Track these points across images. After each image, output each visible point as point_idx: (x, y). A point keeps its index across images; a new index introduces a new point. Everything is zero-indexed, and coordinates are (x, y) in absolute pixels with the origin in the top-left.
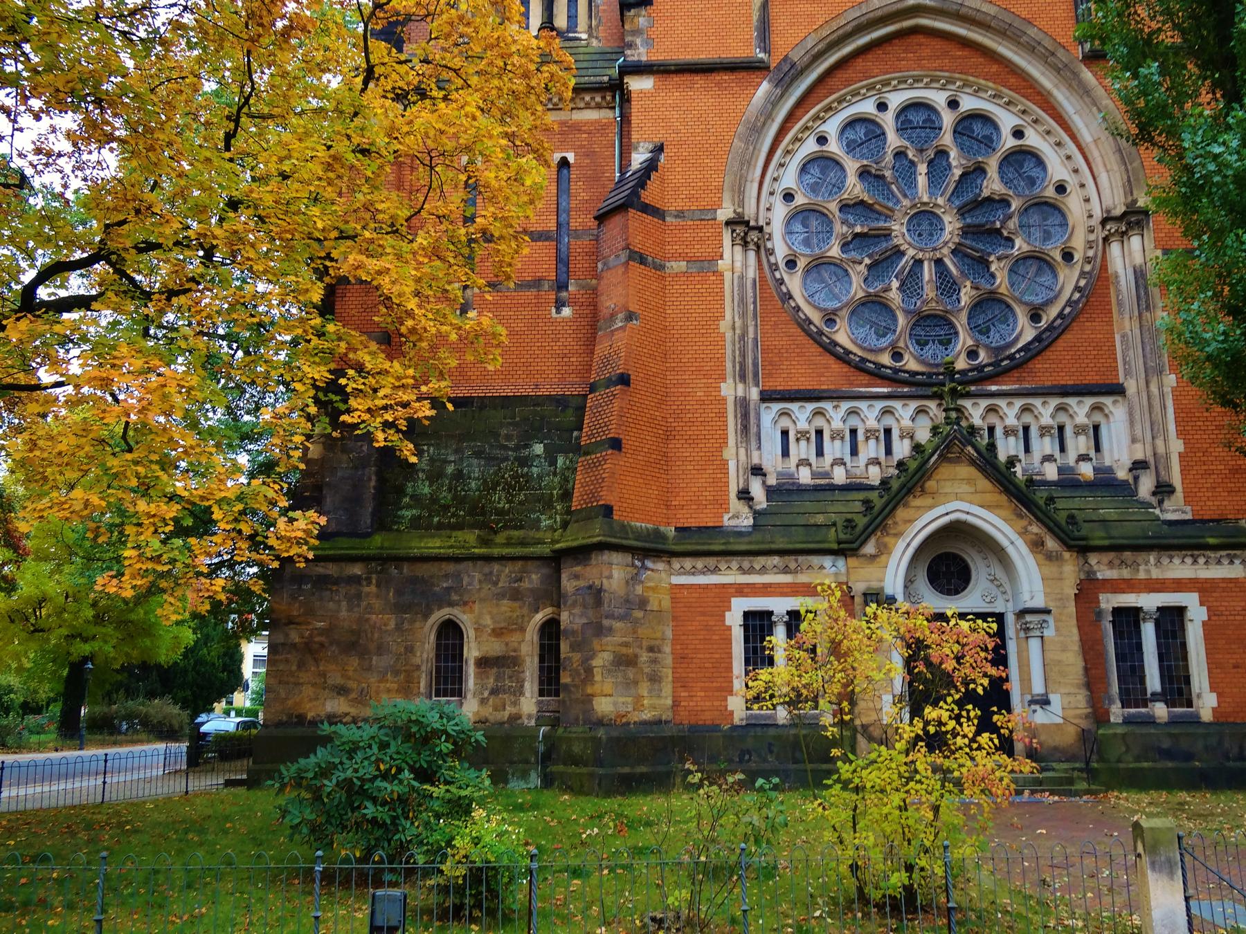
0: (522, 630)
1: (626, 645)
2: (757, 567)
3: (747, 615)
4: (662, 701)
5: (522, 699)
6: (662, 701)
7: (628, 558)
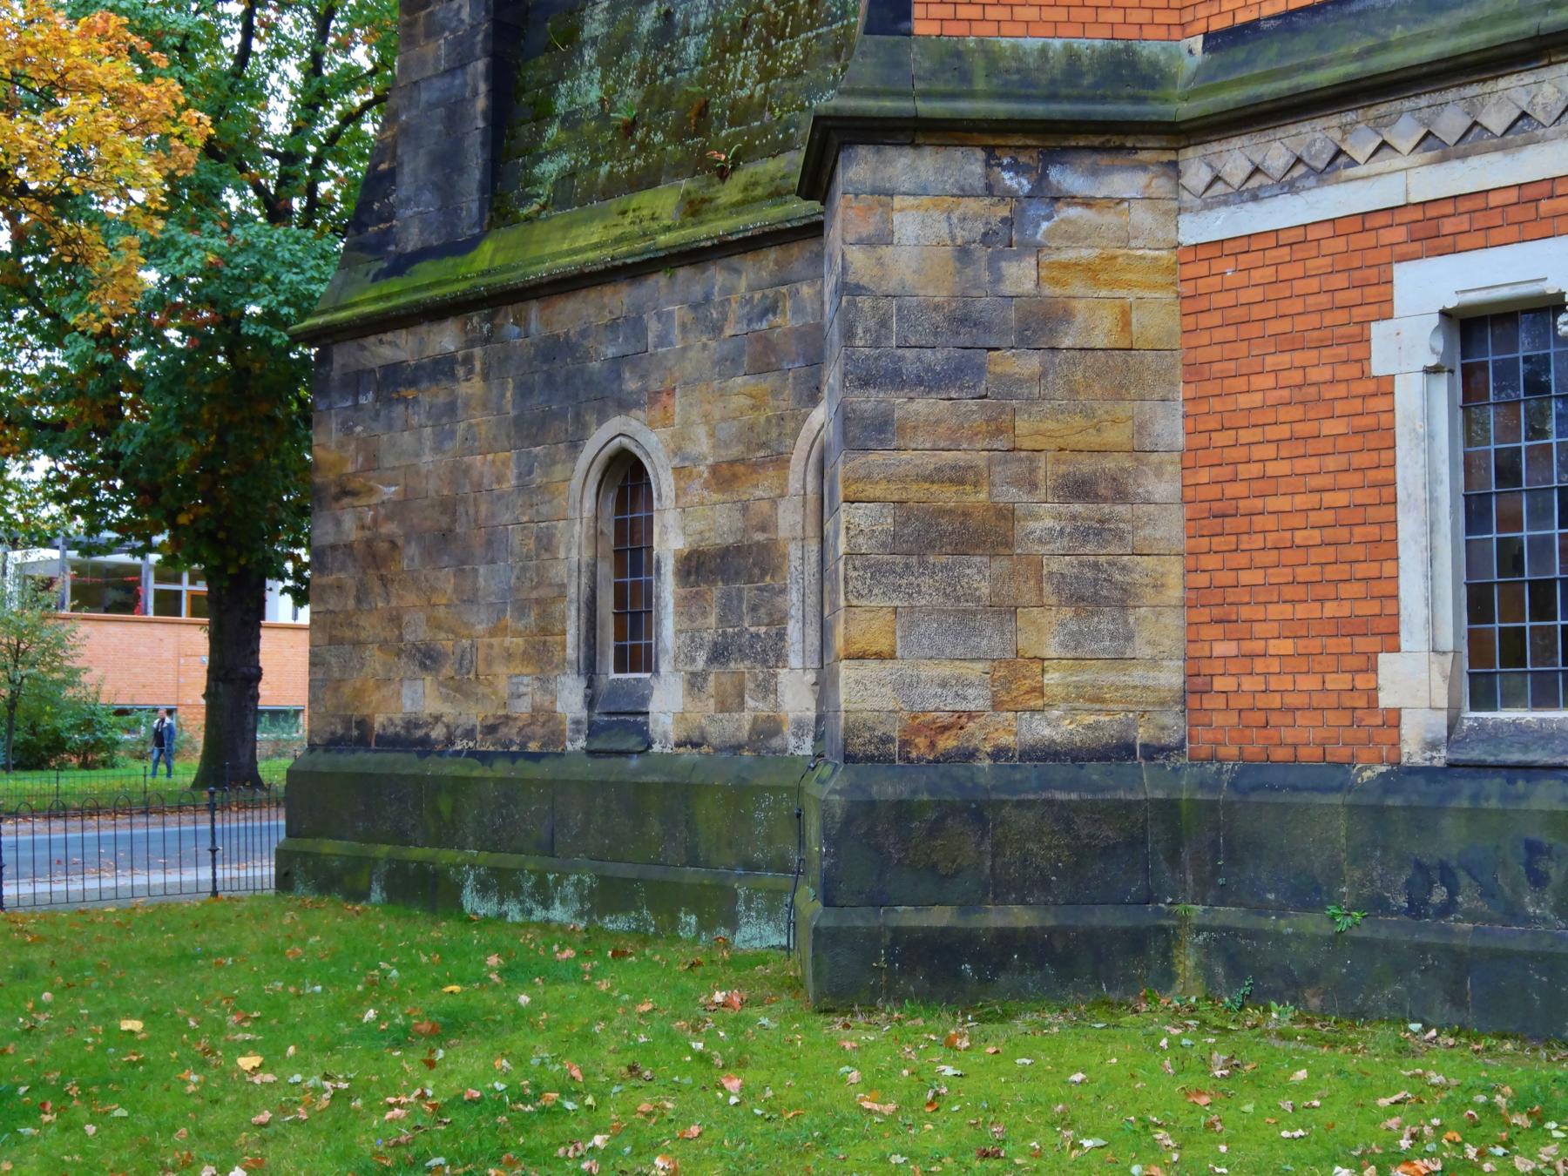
0: (780, 461)
1: (958, 477)
2: (1496, 121)
3: (1470, 326)
4: (1136, 676)
5: (782, 672)
6: (1136, 676)
7: (970, 165)
